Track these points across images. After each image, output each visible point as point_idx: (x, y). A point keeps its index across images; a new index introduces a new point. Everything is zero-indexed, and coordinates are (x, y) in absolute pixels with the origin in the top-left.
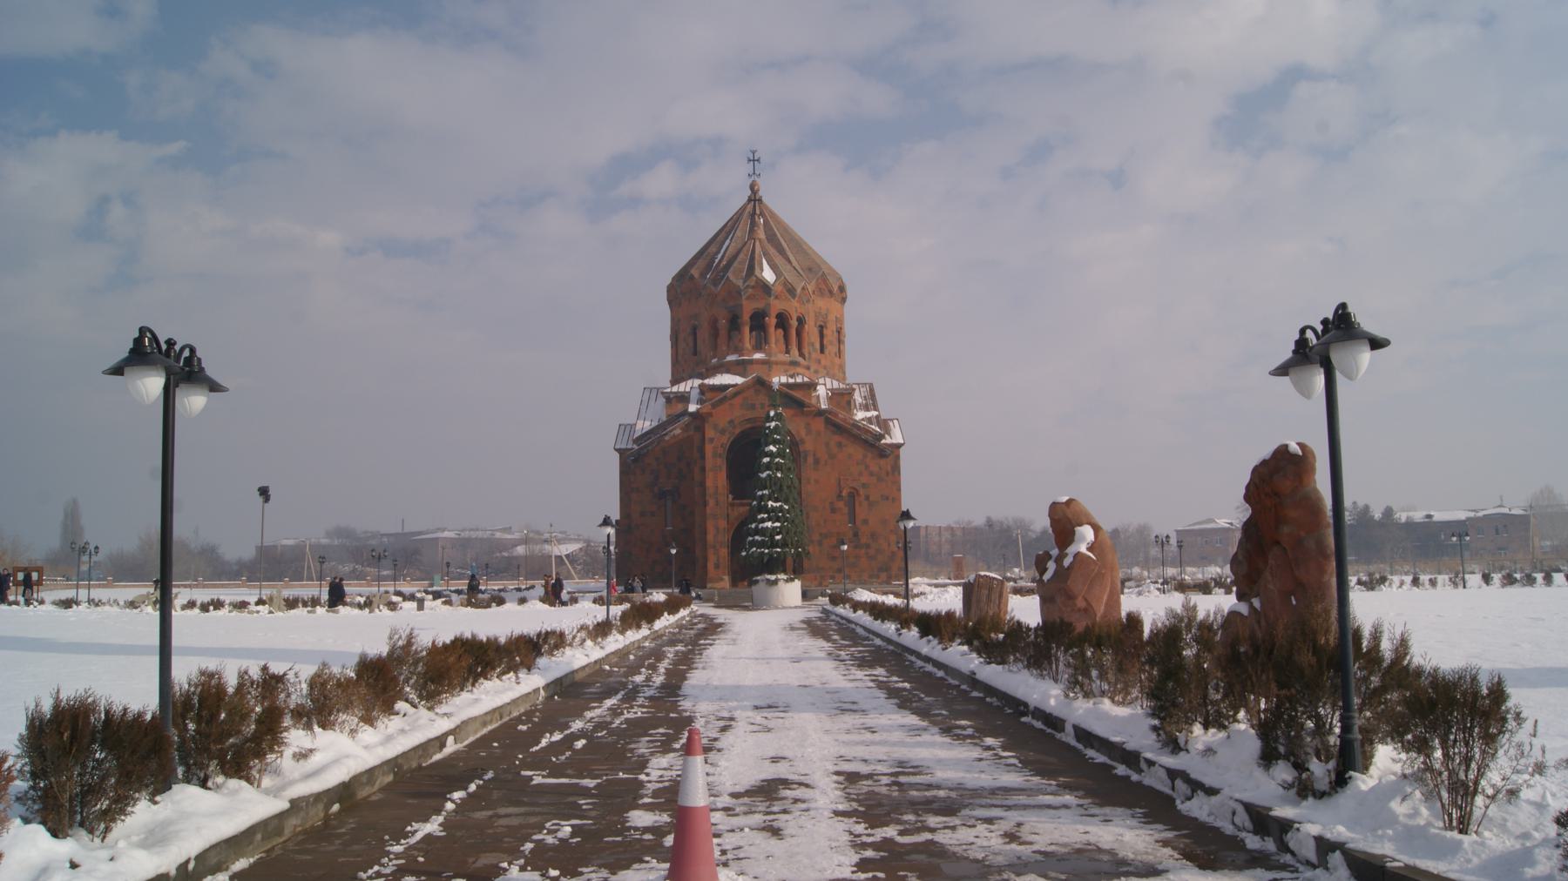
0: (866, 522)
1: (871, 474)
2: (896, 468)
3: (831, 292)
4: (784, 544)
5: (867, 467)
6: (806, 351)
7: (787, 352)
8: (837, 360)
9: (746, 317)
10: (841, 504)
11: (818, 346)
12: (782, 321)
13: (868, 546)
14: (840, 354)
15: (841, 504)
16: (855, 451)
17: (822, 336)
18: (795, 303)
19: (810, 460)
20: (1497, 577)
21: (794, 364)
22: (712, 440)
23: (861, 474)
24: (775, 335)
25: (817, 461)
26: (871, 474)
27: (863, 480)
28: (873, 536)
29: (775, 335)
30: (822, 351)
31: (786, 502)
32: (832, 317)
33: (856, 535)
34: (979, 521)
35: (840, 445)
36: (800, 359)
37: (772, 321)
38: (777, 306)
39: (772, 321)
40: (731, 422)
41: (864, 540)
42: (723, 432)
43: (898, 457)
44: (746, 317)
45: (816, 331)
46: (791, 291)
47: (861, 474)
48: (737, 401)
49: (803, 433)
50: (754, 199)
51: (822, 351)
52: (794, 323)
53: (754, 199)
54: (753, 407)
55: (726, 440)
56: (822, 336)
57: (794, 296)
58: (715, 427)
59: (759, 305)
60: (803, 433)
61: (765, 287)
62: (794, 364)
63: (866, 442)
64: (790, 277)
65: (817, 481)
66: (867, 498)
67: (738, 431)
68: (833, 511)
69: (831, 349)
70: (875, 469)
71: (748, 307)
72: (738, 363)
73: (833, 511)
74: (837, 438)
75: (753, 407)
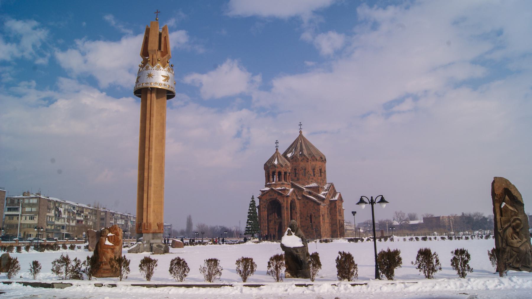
0: (314, 222)
3: (317, 160)
4: (251, 231)
11: (312, 174)
12: (280, 173)
18: (283, 169)
20: (420, 237)
21: (283, 184)
30: (314, 175)
34: (459, 214)
35: (307, 202)
46: (282, 166)
48: (268, 194)
50: (301, 135)
51: (314, 175)
52: (283, 174)
53: (301, 135)
54: (271, 196)
59: (273, 170)
61: (274, 166)
64: (281, 162)
68: (306, 220)
71: (271, 171)
72: (269, 185)
73: (306, 220)
74: (307, 201)
75: (271, 196)
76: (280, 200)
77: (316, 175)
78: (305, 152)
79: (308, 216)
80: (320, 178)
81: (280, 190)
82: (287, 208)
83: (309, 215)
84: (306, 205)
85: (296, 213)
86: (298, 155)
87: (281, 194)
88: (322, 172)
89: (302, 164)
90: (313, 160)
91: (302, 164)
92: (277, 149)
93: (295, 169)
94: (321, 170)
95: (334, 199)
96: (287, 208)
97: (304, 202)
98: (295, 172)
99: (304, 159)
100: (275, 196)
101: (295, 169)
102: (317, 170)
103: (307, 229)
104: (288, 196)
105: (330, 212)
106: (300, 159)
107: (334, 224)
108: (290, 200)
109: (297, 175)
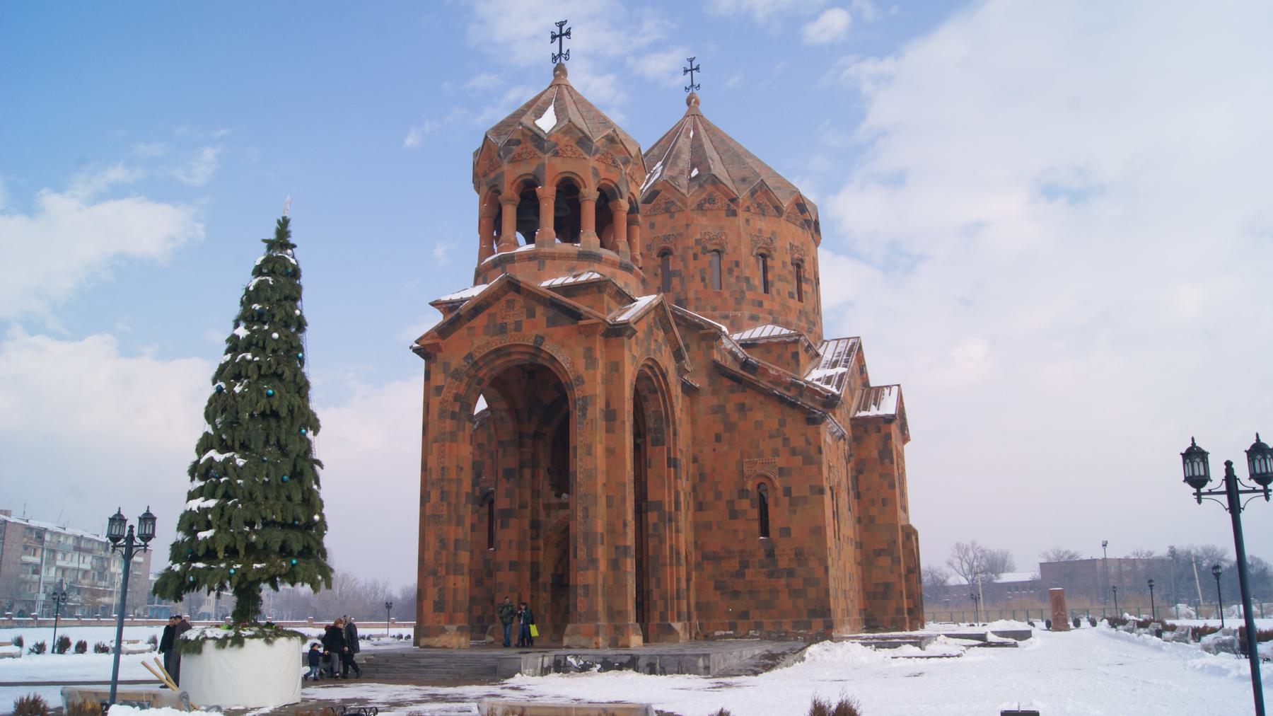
0: (786, 532)
1: (794, 452)
3: (778, 209)
5: (786, 441)
10: (745, 504)
11: (757, 281)
12: (569, 190)
13: (791, 573)
15: (745, 504)
18: (592, 162)
23: (776, 453)
26: (794, 452)
27: (781, 461)
28: (799, 555)
30: (766, 286)
31: (244, 448)
33: (770, 554)
34: (1161, 551)
35: (742, 408)
37: (547, 194)
39: (547, 194)
40: (470, 356)
41: (783, 563)
42: (456, 375)
46: (584, 141)
48: (480, 321)
49: (581, 364)
59: (527, 169)
61: (537, 138)
63: (781, 399)
66: (788, 492)
68: (734, 515)
71: (511, 174)
74: (739, 397)
75: (502, 329)
77: (777, 286)
78: (718, 169)
79: (743, 493)
80: (794, 303)
81: (566, 290)
82: (611, 415)
83: (750, 486)
84: (730, 427)
85: (673, 463)
86: (683, 181)
87: (575, 315)
88: (803, 276)
89: (704, 225)
90: (763, 212)
91: (704, 225)
92: (559, 59)
93: (665, 253)
94: (798, 265)
95: (873, 412)
96: (611, 415)
97: (719, 410)
98: (665, 267)
99: (711, 200)
100: (533, 329)
101: (665, 253)
102: (781, 262)
103: (740, 574)
104: (618, 332)
105: (856, 481)
106: (691, 195)
107: (879, 553)
108: (631, 361)
109: (675, 281)
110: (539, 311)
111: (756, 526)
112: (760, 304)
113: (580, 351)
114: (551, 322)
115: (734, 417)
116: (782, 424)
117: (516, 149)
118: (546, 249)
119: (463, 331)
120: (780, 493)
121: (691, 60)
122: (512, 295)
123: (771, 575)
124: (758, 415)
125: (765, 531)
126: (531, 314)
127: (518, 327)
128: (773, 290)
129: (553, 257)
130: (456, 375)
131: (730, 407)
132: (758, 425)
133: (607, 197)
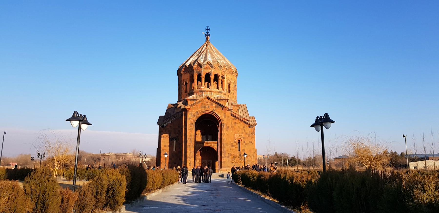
0: (244, 150)
2: (253, 133)
5: (245, 131)
6: (223, 88)
7: (218, 88)
8: (234, 96)
9: (203, 76)
10: (235, 144)
12: (216, 76)
14: (235, 94)
16: (241, 125)
17: (229, 87)
19: (225, 127)
22: (190, 118)
23: (242, 133)
24: (213, 84)
25: (228, 127)
26: (246, 134)
27: (243, 136)
29: (213, 84)
30: (229, 92)
32: (233, 81)
34: (272, 154)
36: (223, 91)
37: (212, 77)
38: (213, 72)
39: (212, 77)
40: (197, 112)
42: (194, 115)
43: (254, 129)
44: (203, 76)
45: (227, 85)
46: (220, 66)
47: (242, 133)
48: (199, 104)
49: (223, 117)
51: (229, 92)
52: (220, 78)
54: (205, 107)
55: (195, 119)
56: (229, 87)
57: (221, 68)
58: (191, 114)
60: (223, 117)
62: (220, 92)
65: (227, 134)
66: (244, 142)
67: (199, 116)
69: (232, 92)
70: (247, 132)
71: (204, 72)
73: (233, 146)
75: (205, 107)
76: (220, 113)
83: (237, 140)
87: (222, 106)
90: (230, 73)
110: (214, 104)
111: (237, 149)
112: (228, 96)
113: (223, 114)
114: (216, 107)
115: (233, 125)
116: (244, 127)
117: (205, 66)
118: (213, 90)
119: (195, 106)
120: (243, 142)
121: (208, 27)
122: (207, 100)
123: (240, 159)
124: (239, 125)
125: (239, 151)
126: (212, 105)
127: (209, 106)
128: (231, 92)
129: (214, 92)
130: (194, 115)
131: (233, 123)
132: (239, 127)
133: (216, 76)
